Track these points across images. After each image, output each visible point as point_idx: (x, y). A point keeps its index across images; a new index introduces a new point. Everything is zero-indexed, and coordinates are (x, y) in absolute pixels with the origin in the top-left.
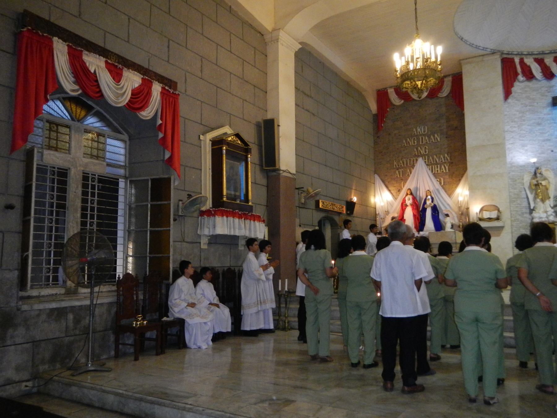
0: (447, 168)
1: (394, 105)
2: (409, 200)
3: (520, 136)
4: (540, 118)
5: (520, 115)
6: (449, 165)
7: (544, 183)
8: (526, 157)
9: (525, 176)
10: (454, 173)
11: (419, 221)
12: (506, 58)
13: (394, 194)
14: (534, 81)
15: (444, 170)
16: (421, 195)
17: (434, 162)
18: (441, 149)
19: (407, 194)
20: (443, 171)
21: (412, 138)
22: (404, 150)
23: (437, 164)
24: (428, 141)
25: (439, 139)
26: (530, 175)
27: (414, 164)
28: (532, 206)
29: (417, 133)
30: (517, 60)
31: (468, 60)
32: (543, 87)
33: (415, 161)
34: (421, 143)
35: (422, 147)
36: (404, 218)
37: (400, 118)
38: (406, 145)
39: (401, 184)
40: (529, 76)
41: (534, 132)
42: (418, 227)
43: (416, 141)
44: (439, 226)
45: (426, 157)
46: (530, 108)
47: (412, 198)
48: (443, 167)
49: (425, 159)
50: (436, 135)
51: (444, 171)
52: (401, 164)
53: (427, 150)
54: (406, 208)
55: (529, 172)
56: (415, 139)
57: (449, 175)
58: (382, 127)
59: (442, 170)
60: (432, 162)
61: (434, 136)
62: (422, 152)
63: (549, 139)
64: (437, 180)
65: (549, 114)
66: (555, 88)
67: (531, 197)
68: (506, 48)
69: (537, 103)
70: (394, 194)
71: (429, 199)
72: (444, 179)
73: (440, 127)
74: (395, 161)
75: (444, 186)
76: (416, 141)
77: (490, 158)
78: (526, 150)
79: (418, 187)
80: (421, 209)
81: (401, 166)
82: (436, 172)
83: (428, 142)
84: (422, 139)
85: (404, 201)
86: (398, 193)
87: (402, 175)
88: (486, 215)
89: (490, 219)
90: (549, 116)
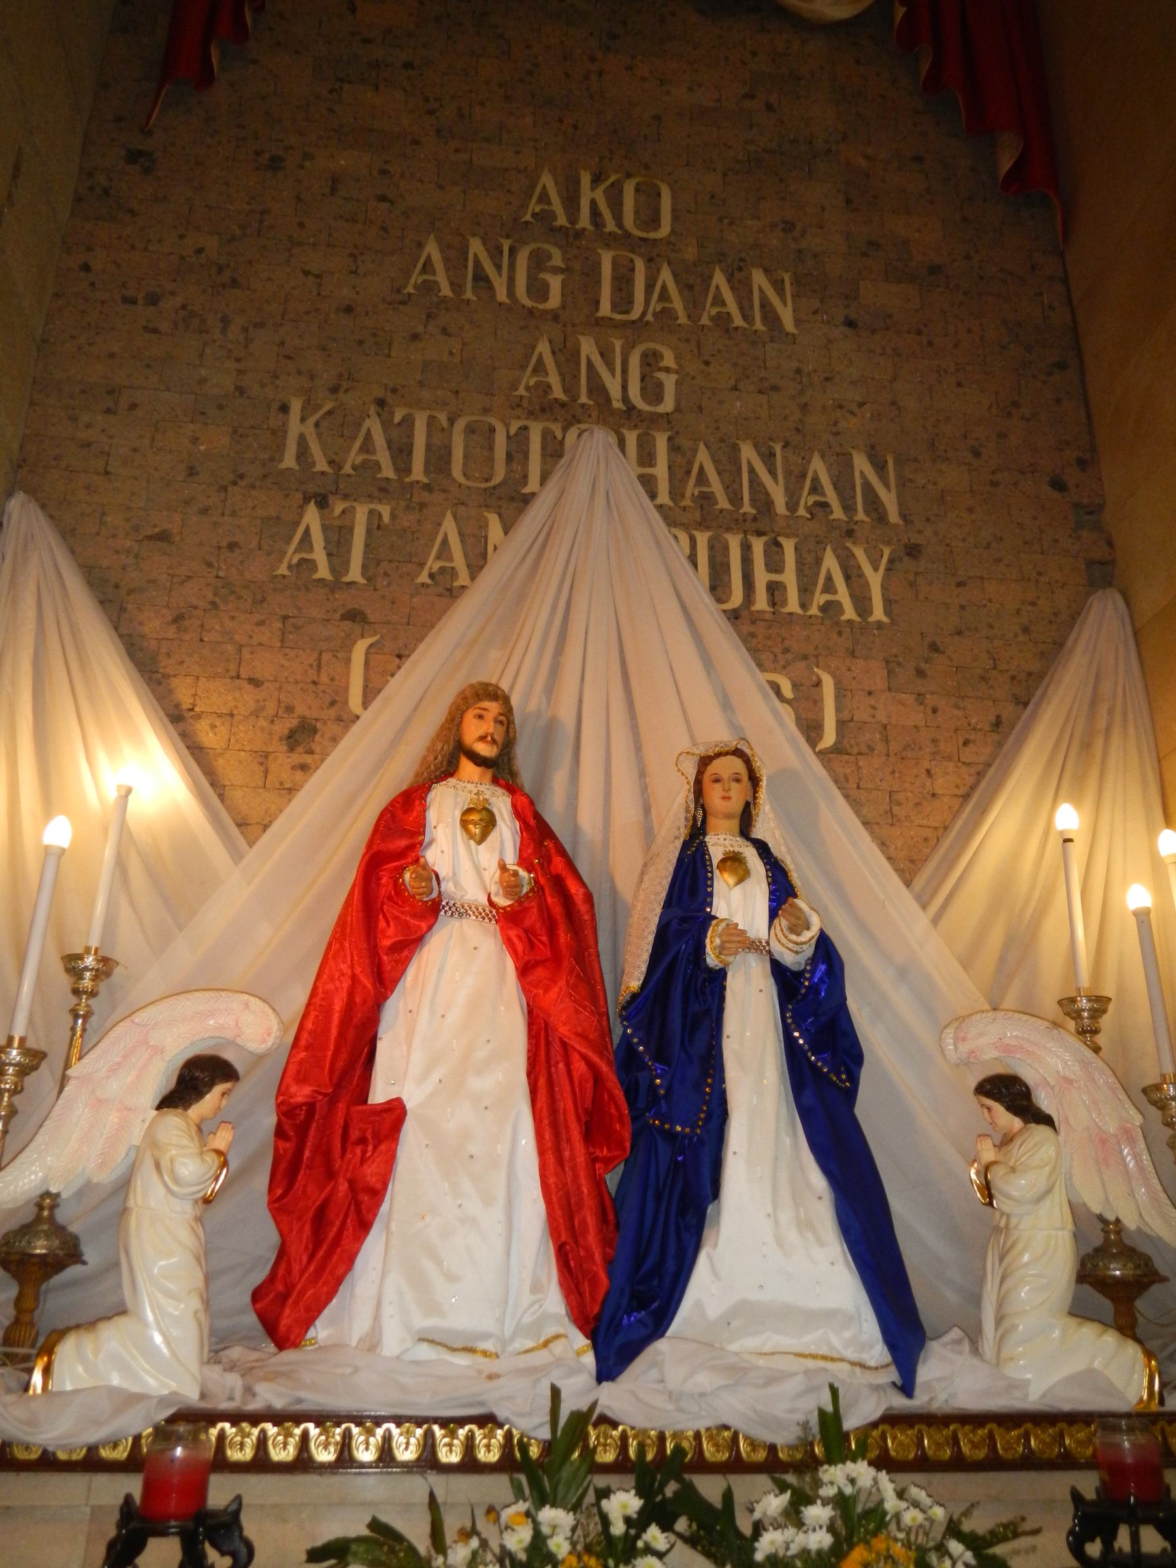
0: (875, 580)
13: (232, 770)
15: (843, 594)
16: (588, 818)
17: (735, 498)
20: (830, 608)
21: (513, 251)
24: (677, 304)
29: (573, 218)
34: (605, 309)
36: (379, 1094)
37: (408, 65)
39: (348, 661)
43: (555, 283)
45: (661, 443)
48: (830, 563)
50: (759, 278)
51: (849, 613)
53: (669, 382)
54: (410, 943)
56: (549, 257)
59: (820, 598)
60: (723, 503)
62: (614, 387)
70: (232, 770)
71: (733, 861)
74: (296, 406)
76: (555, 283)
82: (761, 602)
86: (282, 762)
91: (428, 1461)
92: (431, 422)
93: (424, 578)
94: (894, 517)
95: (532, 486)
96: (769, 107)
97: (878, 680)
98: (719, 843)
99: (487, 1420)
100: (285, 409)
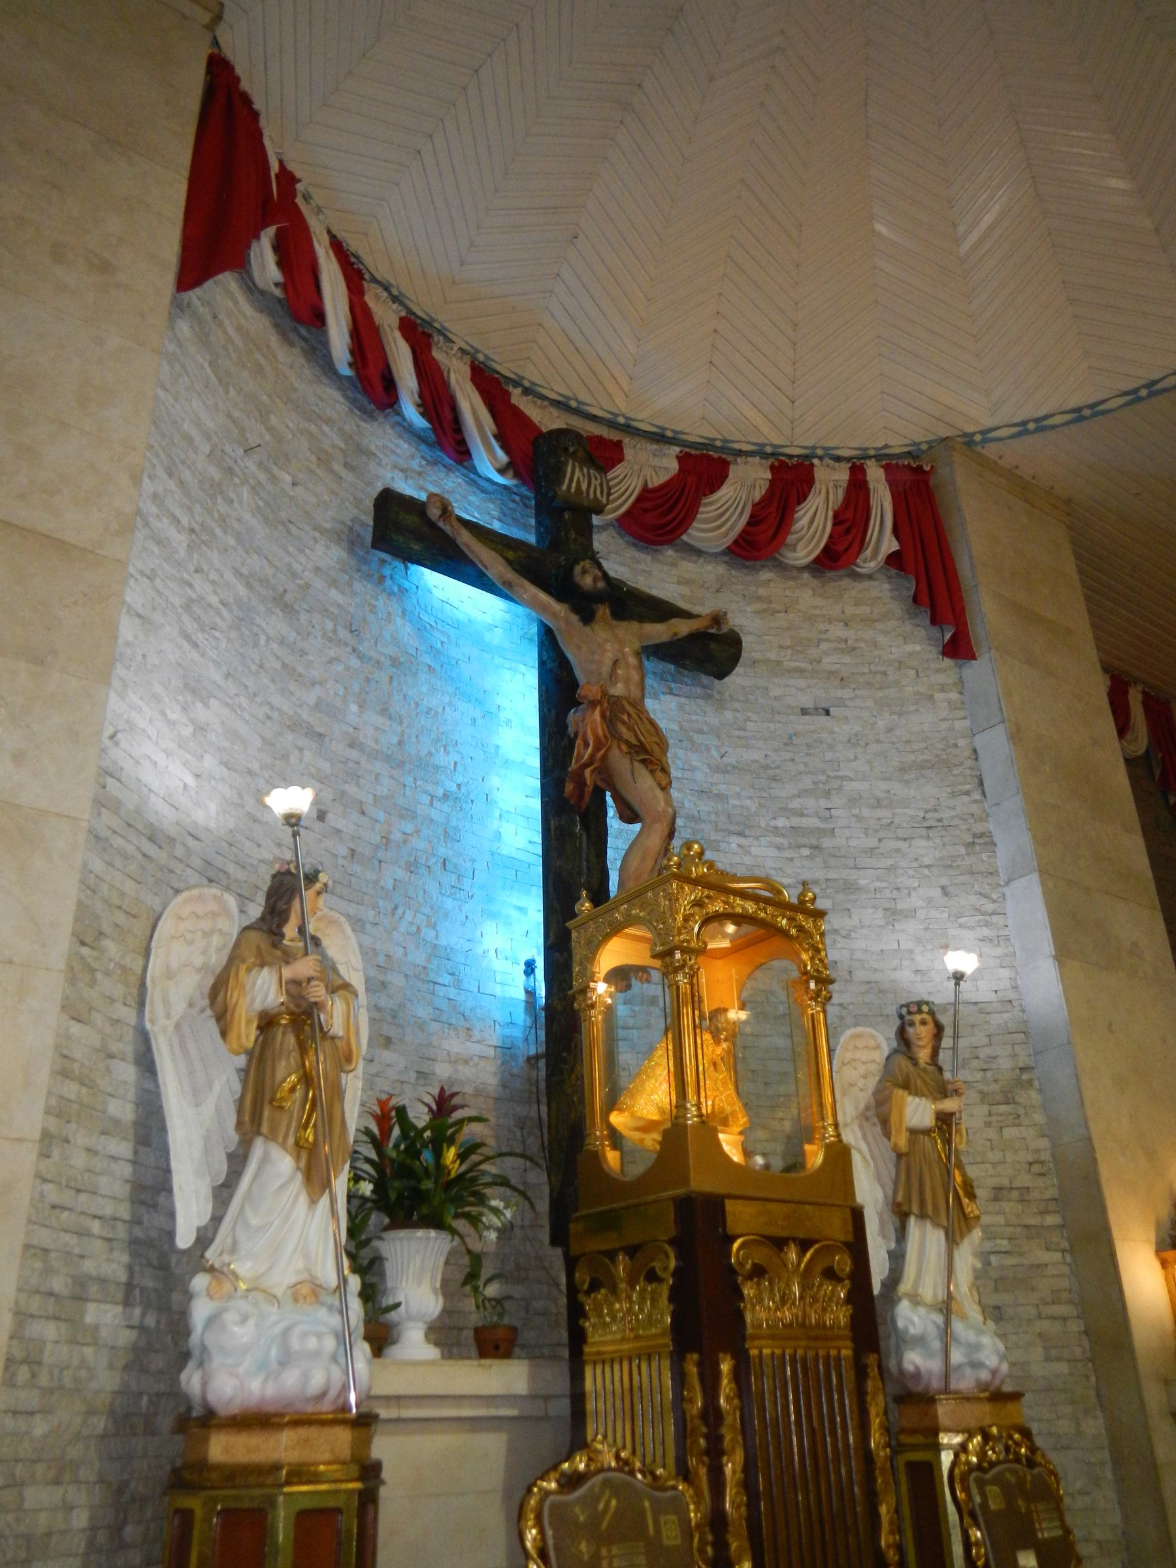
3: (187, 607)
7: (335, 1016)
8: (190, 780)
9: (165, 927)
26: (206, 925)
63: (321, 730)
65: (334, 583)
66: (372, 466)
69: (294, 484)
78: (201, 729)
90: (334, 594)
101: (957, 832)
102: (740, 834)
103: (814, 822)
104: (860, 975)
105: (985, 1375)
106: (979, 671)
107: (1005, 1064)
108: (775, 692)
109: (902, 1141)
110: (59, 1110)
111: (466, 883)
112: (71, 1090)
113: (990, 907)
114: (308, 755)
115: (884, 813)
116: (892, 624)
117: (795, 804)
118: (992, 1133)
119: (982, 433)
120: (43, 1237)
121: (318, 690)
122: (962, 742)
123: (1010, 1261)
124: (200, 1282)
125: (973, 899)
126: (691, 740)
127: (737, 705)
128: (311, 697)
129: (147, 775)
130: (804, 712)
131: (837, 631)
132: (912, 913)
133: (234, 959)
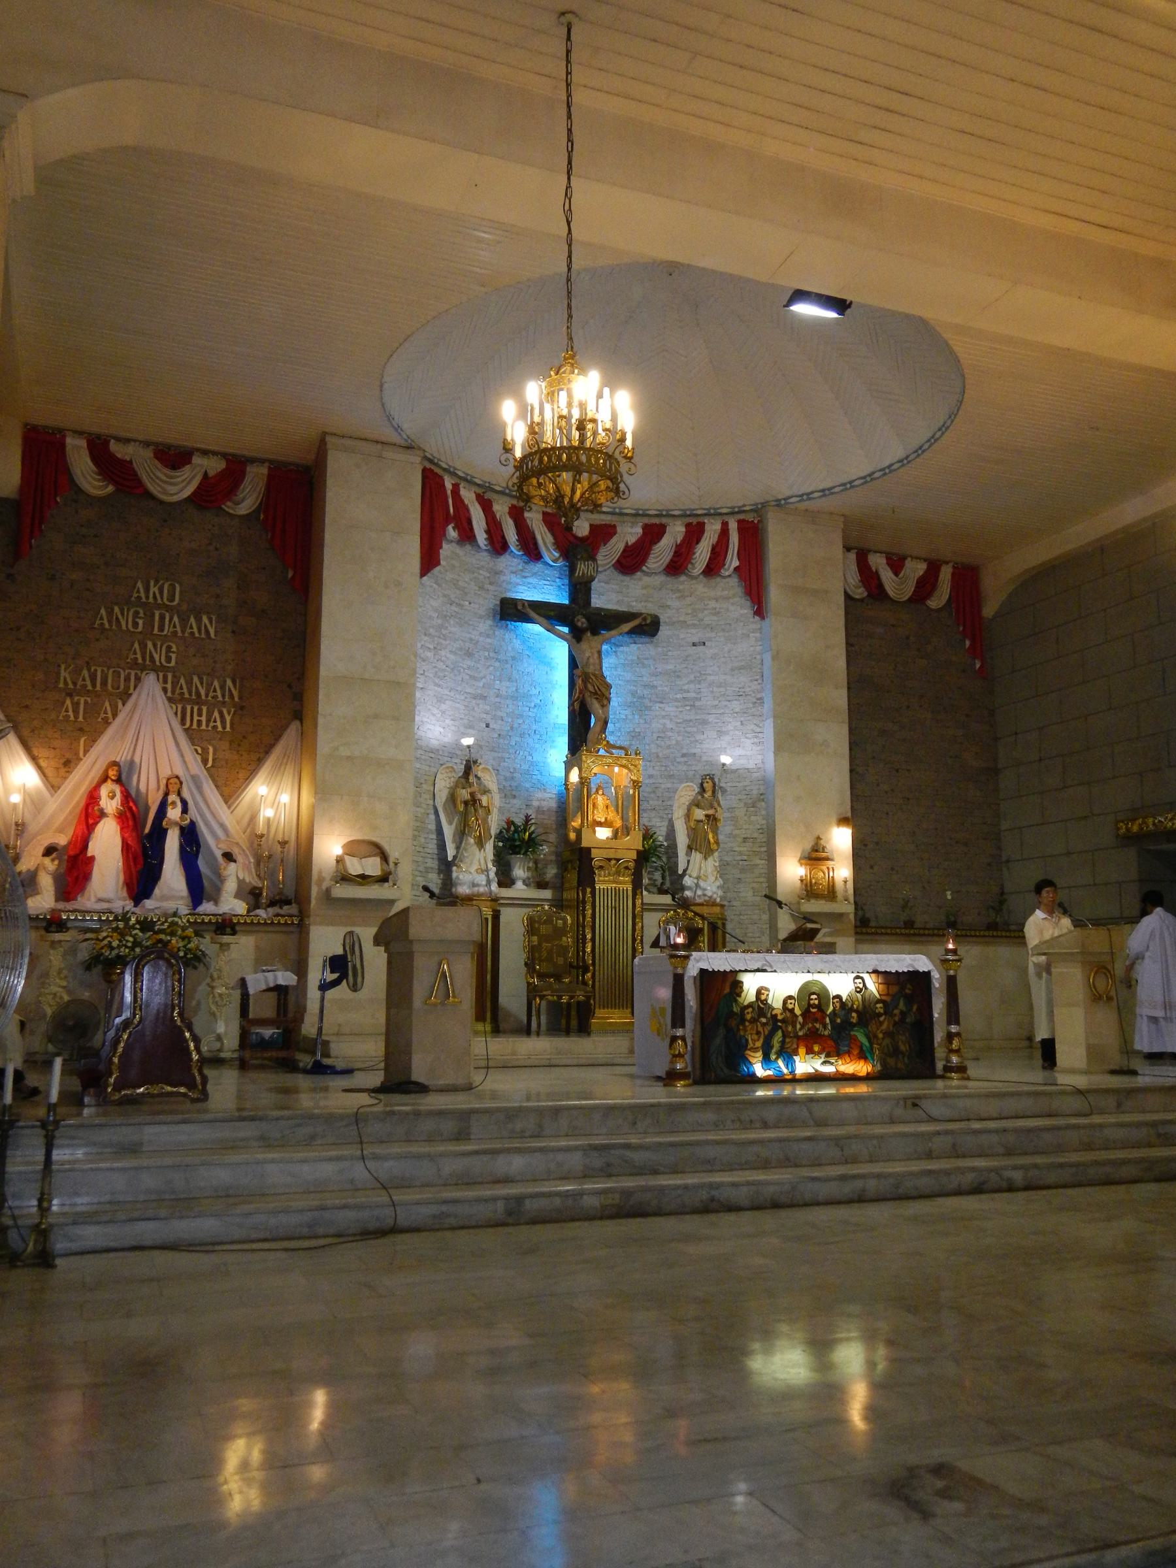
0: (228, 719)
1: (79, 490)
2: (112, 798)
3: (436, 674)
4: (471, 640)
5: (439, 621)
6: (234, 714)
7: (484, 800)
8: (442, 730)
10: (244, 737)
11: (140, 867)
12: (431, 471)
13: (50, 772)
14: (468, 547)
15: (219, 724)
17: (190, 694)
18: (215, 662)
19: (105, 779)
20: (215, 727)
21: (128, 610)
22: (98, 640)
23: (199, 701)
24: (178, 629)
25: (212, 632)
26: (450, 775)
27: (127, 688)
28: (451, 852)
29: (147, 597)
30: (448, 486)
31: (348, 442)
32: (483, 567)
33: (133, 678)
35: (159, 644)
36: (89, 854)
38: (107, 626)
40: (467, 535)
41: (459, 671)
42: (135, 887)
43: (141, 622)
44: (197, 890)
46: (456, 609)
47: (122, 792)
48: (216, 714)
49: (165, 681)
50: (205, 619)
51: (220, 729)
52: (84, 680)
53: (173, 656)
54: (96, 823)
55: (448, 768)
57: (231, 742)
58: (31, 547)
60: (187, 696)
61: (199, 620)
62: (156, 657)
64: (196, 750)
65: (488, 636)
66: (502, 578)
67: (449, 831)
68: (432, 449)
70: (50, 772)
71: (174, 803)
72: (214, 754)
73: (218, 596)
75: (213, 770)
76: (141, 622)
77: (376, 716)
78: (443, 712)
79: (137, 760)
80: (147, 830)
81: (85, 686)
82: (195, 726)
83: (180, 634)
84: (162, 618)
85: (93, 798)
86: (63, 770)
87: (85, 712)
88: (355, 867)
89: (364, 879)
90: (489, 640)
91: (100, 920)
92: (102, 671)
93: (100, 720)
94: (236, 699)
95: (131, 691)
96: (216, 549)
97: (227, 745)
98: (172, 797)
99: (111, 912)
100: (59, 666)
101: (749, 697)
102: (662, 703)
103: (693, 695)
104: (704, 758)
105: (707, 898)
106: (771, 623)
107: (755, 792)
108: (682, 636)
109: (692, 824)
110: (417, 829)
111: (544, 737)
112: (419, 824)
113: (758, 730)
114: (481, 706)
115: (722, 689)
116: (736, 599)
117: (686, 687)
118: (746, 818)
119: (784, 499)
120: (415, 859)
121: (484, 680)
122: (758, 657)
123: (745, 863)
124: (454, 868)
125: (752, 726)
126: (643, 664)
127: (665, 644)
128: (481, 684)
129: (430, 735)
130: (694, 645)
131: (712, 604)
132: (726, 733)
133: (456, 785)
